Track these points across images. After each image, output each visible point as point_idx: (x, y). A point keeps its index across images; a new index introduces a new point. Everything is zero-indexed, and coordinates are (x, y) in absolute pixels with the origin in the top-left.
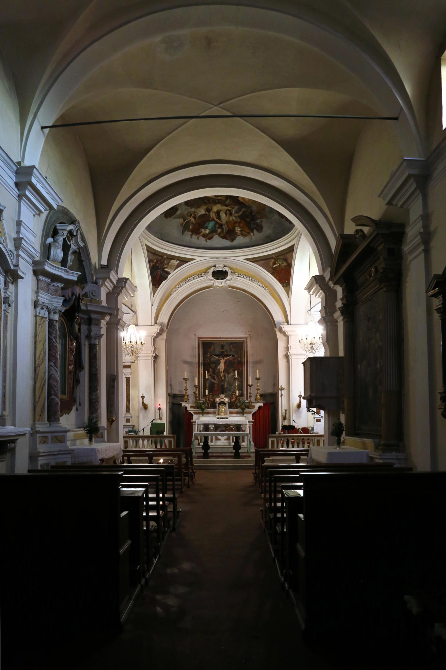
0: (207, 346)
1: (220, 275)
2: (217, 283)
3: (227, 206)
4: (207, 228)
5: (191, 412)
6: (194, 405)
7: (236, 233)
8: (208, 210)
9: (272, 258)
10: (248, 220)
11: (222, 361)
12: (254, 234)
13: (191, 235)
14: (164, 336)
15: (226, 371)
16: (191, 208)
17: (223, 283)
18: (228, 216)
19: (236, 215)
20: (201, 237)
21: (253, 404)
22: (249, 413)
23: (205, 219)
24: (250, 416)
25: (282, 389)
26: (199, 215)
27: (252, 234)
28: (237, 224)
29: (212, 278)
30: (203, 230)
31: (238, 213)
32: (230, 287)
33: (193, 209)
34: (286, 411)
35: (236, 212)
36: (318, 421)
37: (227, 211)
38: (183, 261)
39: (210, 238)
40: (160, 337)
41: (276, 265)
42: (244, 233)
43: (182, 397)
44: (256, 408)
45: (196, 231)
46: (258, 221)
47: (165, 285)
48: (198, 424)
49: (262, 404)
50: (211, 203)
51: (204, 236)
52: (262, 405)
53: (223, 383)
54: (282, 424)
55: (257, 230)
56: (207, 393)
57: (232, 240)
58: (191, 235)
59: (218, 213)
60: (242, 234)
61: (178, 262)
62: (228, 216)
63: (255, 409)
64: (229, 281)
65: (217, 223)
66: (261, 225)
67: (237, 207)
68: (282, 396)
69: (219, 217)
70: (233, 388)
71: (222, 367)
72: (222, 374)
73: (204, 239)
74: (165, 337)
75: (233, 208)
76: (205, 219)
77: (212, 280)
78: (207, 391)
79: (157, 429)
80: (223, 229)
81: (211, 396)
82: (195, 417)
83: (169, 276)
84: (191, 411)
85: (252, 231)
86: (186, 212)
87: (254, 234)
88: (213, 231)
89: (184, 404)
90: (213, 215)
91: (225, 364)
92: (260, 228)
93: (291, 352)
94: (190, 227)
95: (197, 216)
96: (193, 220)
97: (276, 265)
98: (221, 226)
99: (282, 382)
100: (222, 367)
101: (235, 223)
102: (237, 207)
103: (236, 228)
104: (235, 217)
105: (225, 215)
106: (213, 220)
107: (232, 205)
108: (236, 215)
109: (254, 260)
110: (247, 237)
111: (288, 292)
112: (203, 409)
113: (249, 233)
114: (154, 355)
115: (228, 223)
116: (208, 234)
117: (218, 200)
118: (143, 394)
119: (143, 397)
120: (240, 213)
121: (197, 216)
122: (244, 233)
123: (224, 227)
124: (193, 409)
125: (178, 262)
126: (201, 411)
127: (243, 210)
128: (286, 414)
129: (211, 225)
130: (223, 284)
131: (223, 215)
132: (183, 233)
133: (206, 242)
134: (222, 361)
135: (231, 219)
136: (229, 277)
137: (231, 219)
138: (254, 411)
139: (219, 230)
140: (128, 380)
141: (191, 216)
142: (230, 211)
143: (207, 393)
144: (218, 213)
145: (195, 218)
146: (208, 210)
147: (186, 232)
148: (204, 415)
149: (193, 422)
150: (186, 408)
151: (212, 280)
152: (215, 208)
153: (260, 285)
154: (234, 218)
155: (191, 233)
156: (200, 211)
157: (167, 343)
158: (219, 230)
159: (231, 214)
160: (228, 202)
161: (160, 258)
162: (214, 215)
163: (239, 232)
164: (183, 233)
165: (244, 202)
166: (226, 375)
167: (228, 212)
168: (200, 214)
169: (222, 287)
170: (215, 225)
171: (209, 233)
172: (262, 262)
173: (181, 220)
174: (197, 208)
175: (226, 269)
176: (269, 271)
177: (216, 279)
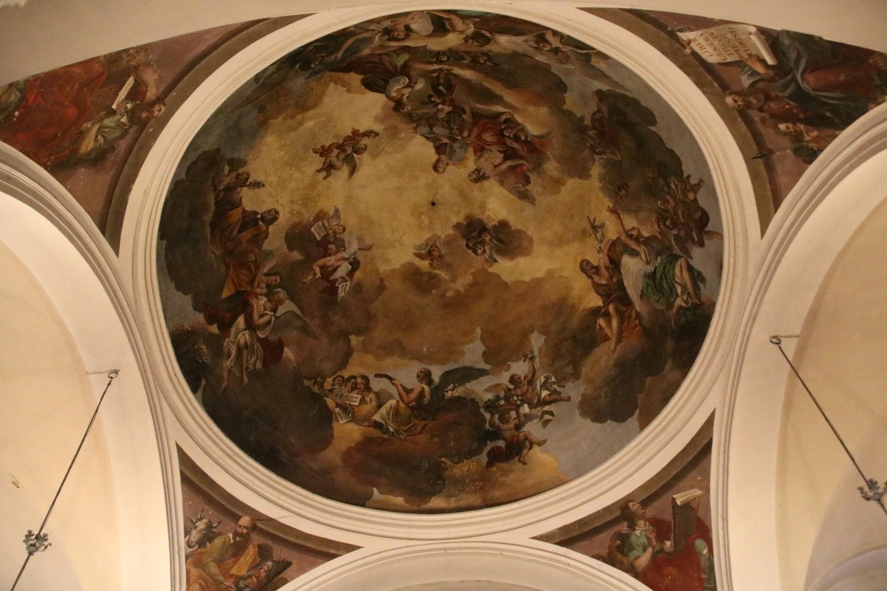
3: (407, 49)
9: (160, 100)
16: (549, 66)
33: (541, 58)
37: (402, 35)
41: (123, 93)
50: (467, 53)
75: (382, 46)
97: (123, 93)
107: (385, 54)
127: (339, 55)
156: (515, 43)
161: (756, 116)
165: (340, 74)
172: (202, 48)
174: (525, 55)
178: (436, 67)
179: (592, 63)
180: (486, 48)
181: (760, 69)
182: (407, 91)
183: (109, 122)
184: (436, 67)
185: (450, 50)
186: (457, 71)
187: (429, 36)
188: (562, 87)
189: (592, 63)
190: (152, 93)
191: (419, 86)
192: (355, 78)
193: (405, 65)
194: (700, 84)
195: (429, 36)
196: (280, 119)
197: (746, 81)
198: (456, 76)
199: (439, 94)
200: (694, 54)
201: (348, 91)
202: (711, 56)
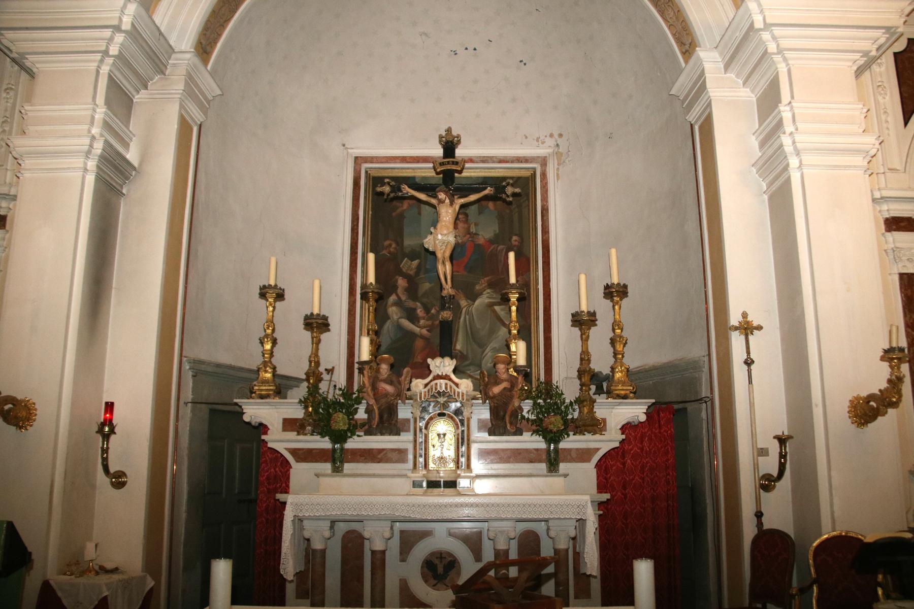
6: (298, 413)
21: (600, 412)
22: (583, 455)
24: (585, 474)
25: (747, 329)
34: (782, 440)
49: (635, 411)
52: (643, 418)
53: (446, 315)
54: (759, 515)
63: (607, 436)
68: (749, 362)
70: (489, 354)
72: (445, 269)
81: (384, 368)
82: (300, 472)
84: (280, 441)
89: (254, 411)
100: (442, 238)
112: (339, 437)
124: (292, 435)
134: (447, 213)
138: (605, 448)
148: (348, 467)
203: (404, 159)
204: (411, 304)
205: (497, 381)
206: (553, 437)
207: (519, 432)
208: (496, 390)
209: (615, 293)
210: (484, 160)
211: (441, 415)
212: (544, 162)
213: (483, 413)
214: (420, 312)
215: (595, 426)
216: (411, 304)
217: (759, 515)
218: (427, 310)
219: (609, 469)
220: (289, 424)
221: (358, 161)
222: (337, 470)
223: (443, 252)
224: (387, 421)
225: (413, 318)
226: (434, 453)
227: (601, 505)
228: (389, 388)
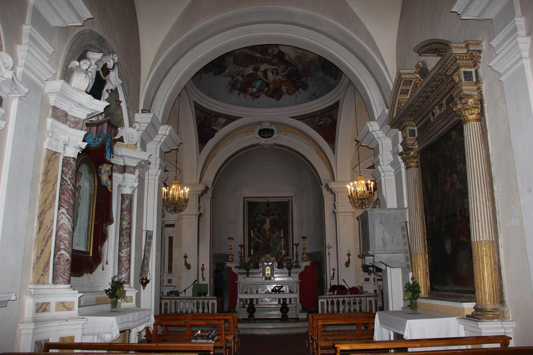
0: (252, 207)
1: (266, 133)
2: (262, 141)
3: (273, 65)
4: (254, 87)
5: (236, 272)
6: (238, 265)
7: (282, 92)
8: (256, 69)
10: (294, 79)
11: (268, 220)
12: (299, 93)
13: (239, 94)
14: (209, 194)
15: (272, 230)
17: (270, 141)
18: (274, 75)
19: (283, 74)
20: (248, 96)
21: (300, 264)
23: (251, 79)
26: (247, 74)
27: (297, 92)
28: (283, 83)
29: (259, 137)
30: (250, 89)
31: (285, 72)
32: (276, 145)
33: (241, 68)
35: (282, 71)
36: (367, 280)
38: (231, 119)
39: (257, 97)
40: (205, 195)
41: (321, 123)
42: (290, 91)
43: (226, 258)
44: (302, 269)
45: (243, 90)
46: (304, 79)
47: (211, 143)
48: (243, 285)
49: (308, 264)
51: (252, 95)
54: (330, 284)
55: (302, 88)
56: (252, 253)
57: (279, 99)
58: (239, 94)
59: (265, 72)
60: (288, 93)
61: (225, 120)
62: (274, 75)
64: (275, 139)
65: (264, 82)
66: (306, 83)
67: (283, 66)
68: (329, 254)
69: (266, 76)
71: (267, 226)
72: (268, 233)
73: (251, 98)
74: (211, 196)
75: (279, 67)
76: (251, 79)
77: (258, 139)
78: (252, 250)
79: (199, 291)
80: (269, 88)
82: (240, 277)
83: (216, 134)
84: (236, 271)
85: (297, 89)
86: (235, 71)
87: (299, 93)
88: (260, 90)
89: (228, 265)
90: (260, 74)
91: (270, 222)
92: (305, 86)
93: (338, 210)
94: (238, 86)
95: (245, 75)
96: (240, 78)
97: (321, 123)
98: (268, 85)
99: (329, 239)
100: (267, 226)
101: (282, 81)
102: (283, 66)
103: (282, 87)
104: (282, 76)
105: (271, 75)
106: (260, 79)
108: (283, 74)
109: (299, 118)
110: (293, 96)
111: (333, 149)
112: (248, 270)
113: (294, 91)
114: (199, 213)
115: (274, 82)
116: (255, 93)
117: (265, 59)
118: (186, 254)
119: (186, 257)
120: (286, 73)
121: (245, 75)
122: (290, 91)
123: (270, 86)
124: (237, 269)
125: (225, 120)
126: (245, 271)
128: (334, 273)
129: (258, 83)
130: (269, 142)
131: (270, 75)
132: (231, 92)
133: (253, 100)
134: (268, 220)
135: (277, 78)
136: (275, 135)
137: (277, 78)
138: (300, 271)
139: (266, 89)
140: (171, 239)
141: (239, 75)
142: (276, 70)
143: (252, 253)
144: (265, 72)
145: (243, 76)
146: (256, 69)
147: (234, 91)
149: (237, 283)
150: (230, 268)
151: (258, 139)
152: (263, 67)
153: (305, 143)
154: (281, 77)
155: (238, 92)
157: (211, 201)
158: (266, 89)
159: (277, 73)
160: (274, 61)
162: (261, 74)
163: (285, 91)
164: (231, 92)
166: (272, 235)
167: (275, 72)
168: (248, 73)
169: (268, 145)
170: (262, 84)
171: (257, 92)
173: (229, 79)
175: (273, 127)
176: (314, 129)
177: (262, 137)
178: (266, 57)
179: (230, 78)
180: (255, 65)
181: (213, 124)
182: (274, 49)
183: (326, 120)
184: (266, 57)
185: (263, 64)
186: (261, 56)
187: (268, 70)
188: (235, 63)
189: (230, 78)
190: (318, 118)
191: (270, 51)
192: (286, 58)
193: (274, 58)
194: (219, 113)
195: (268, 70)
196: (306, 60)
197: (213, 120)
198: (261, 54)
199: (265, 48)
200: (222, 117)
201: (288, 55)
202: (220, 119)
203: (256, 197)
204: (259, 235)
205: (279, 258)
206: (290, 269)
207: (283, 268)
208: (279, 260)
209: (304, 238)
210: (276, 197)
211: (268, 265)
212: (292, 197)
213: (276, 264)
214: (261, 237)
215: (298, 266)
216: (259, 235)
217: (330, 284)
218: (263, 236)
219: (301, 275)
220: (236, 267)
221: (244, 198)
222: (248, 276)
223: (267, 230)
224: (257, 267)
225: (259, 238)
226: (267, 273)
227: (300, 282)
228: (257, 260)
